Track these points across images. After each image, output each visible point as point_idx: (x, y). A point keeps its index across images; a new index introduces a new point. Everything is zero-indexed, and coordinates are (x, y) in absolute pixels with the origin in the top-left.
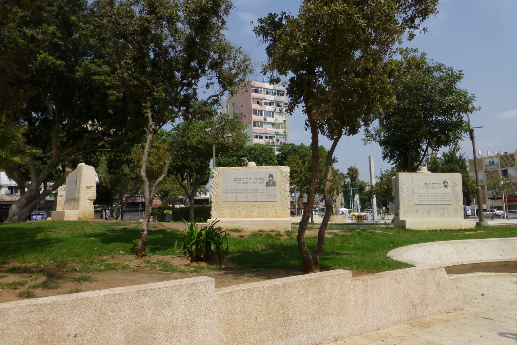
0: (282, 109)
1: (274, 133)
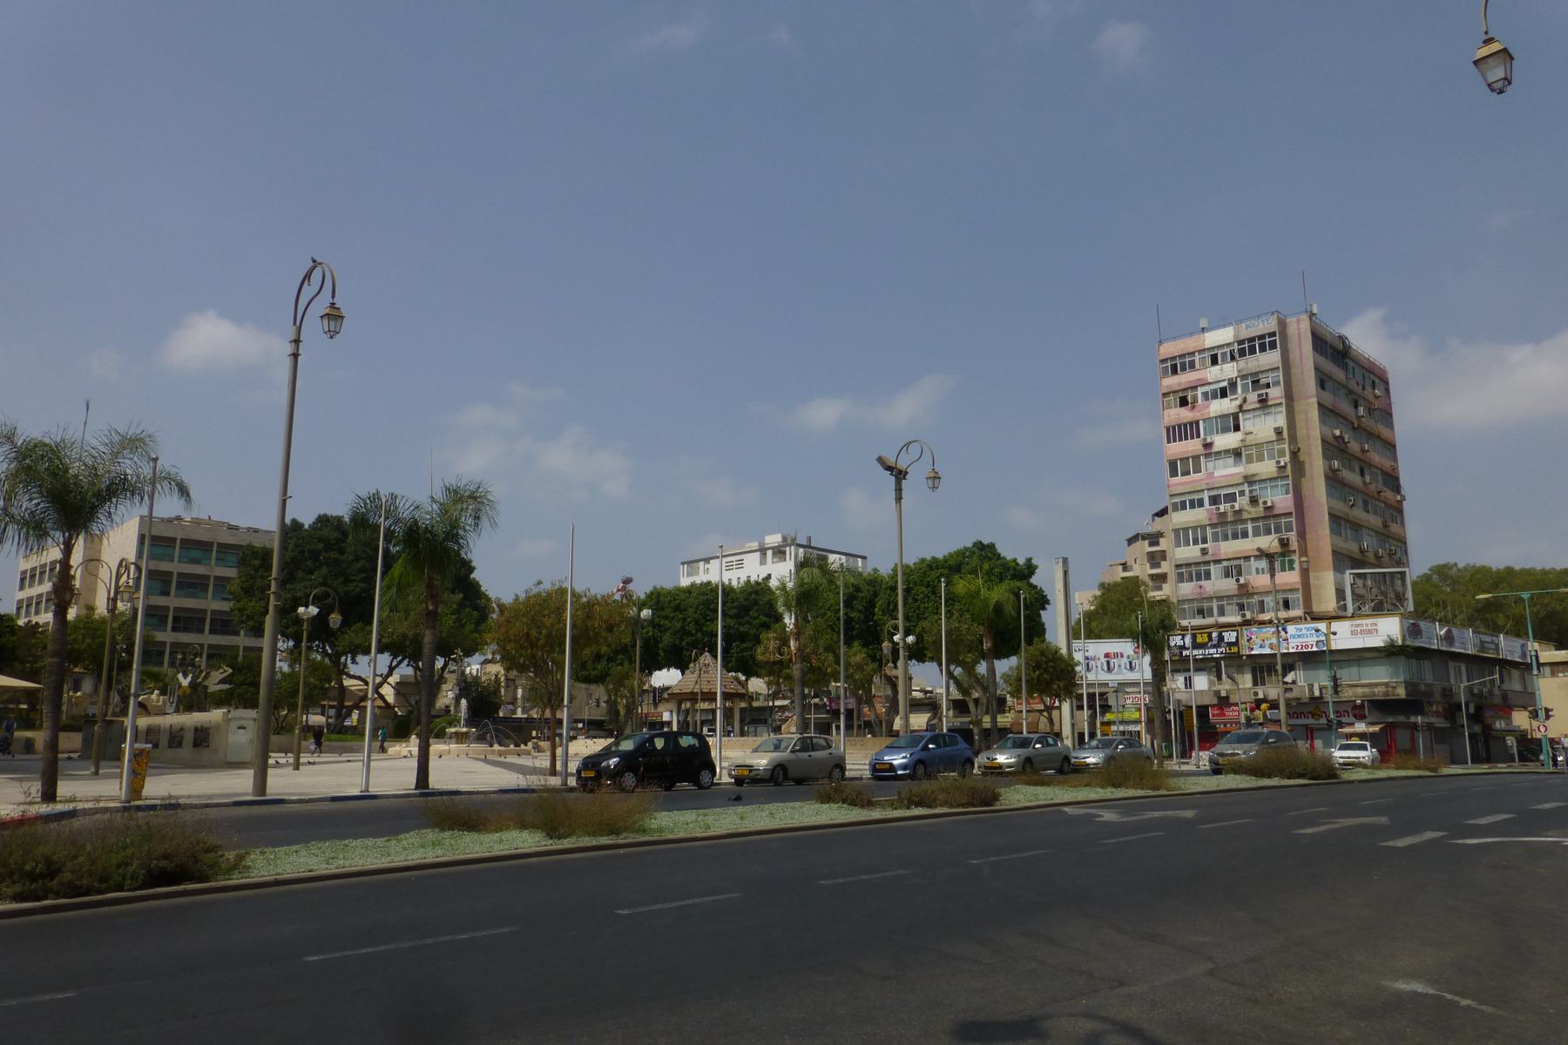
0: (1267, 394)
1: (1241, 481)
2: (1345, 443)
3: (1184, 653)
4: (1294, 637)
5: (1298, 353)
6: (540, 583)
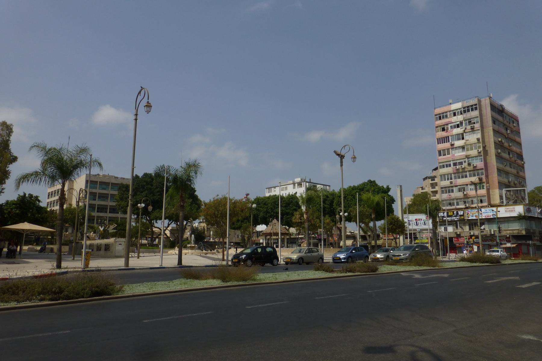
0: (474, 126)
2: (503, 143)
3: (444, 219)
4: (484, 213)
5: (485, 111)
6: (218, 195)
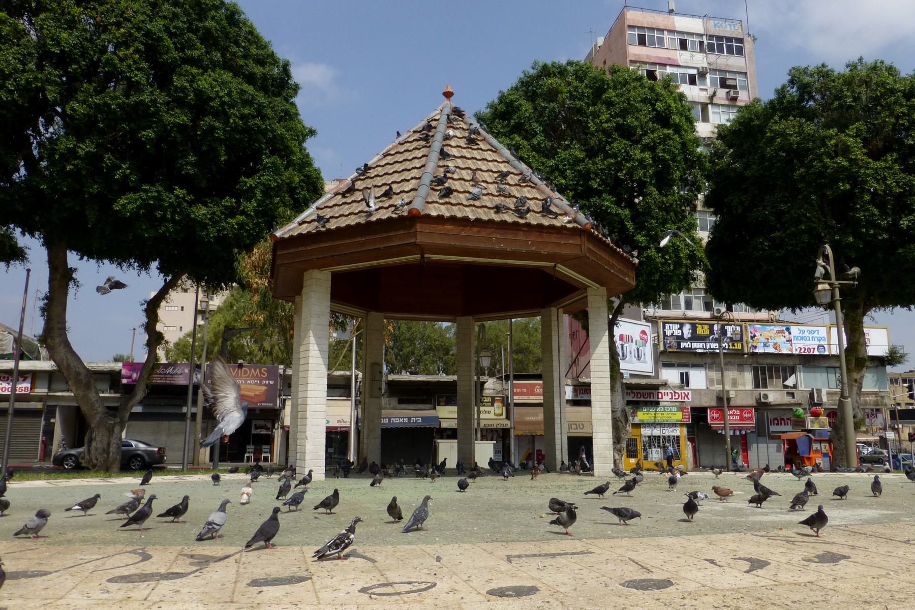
3: (683, 345)
4: (797, 339)
